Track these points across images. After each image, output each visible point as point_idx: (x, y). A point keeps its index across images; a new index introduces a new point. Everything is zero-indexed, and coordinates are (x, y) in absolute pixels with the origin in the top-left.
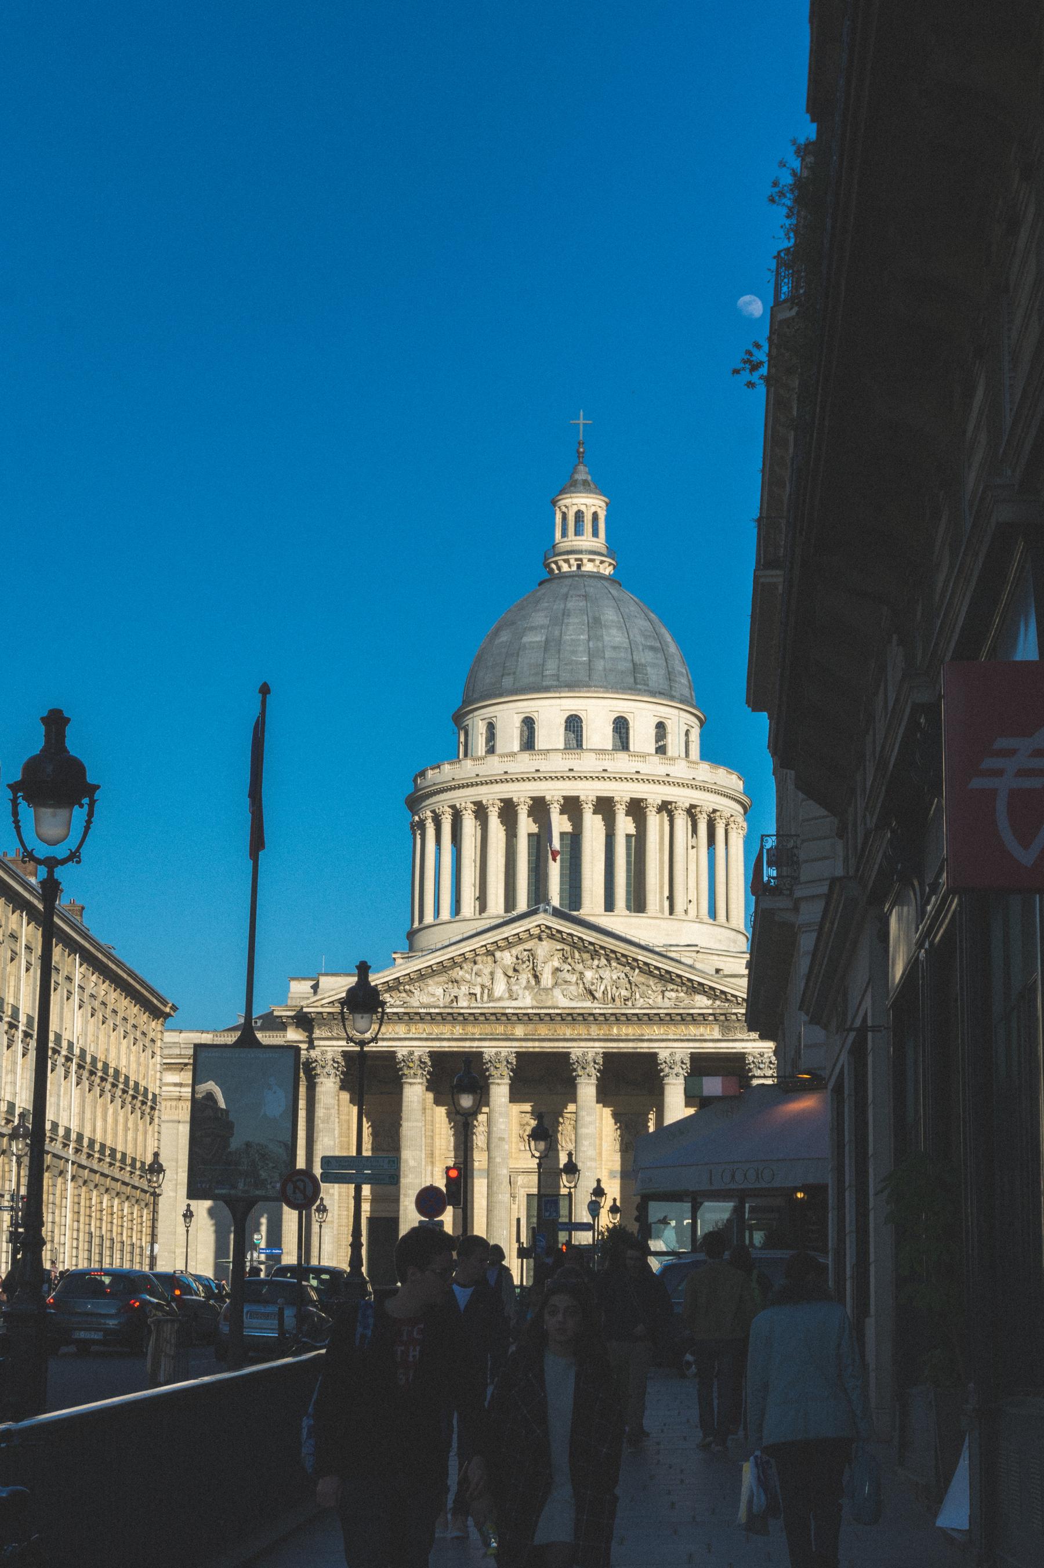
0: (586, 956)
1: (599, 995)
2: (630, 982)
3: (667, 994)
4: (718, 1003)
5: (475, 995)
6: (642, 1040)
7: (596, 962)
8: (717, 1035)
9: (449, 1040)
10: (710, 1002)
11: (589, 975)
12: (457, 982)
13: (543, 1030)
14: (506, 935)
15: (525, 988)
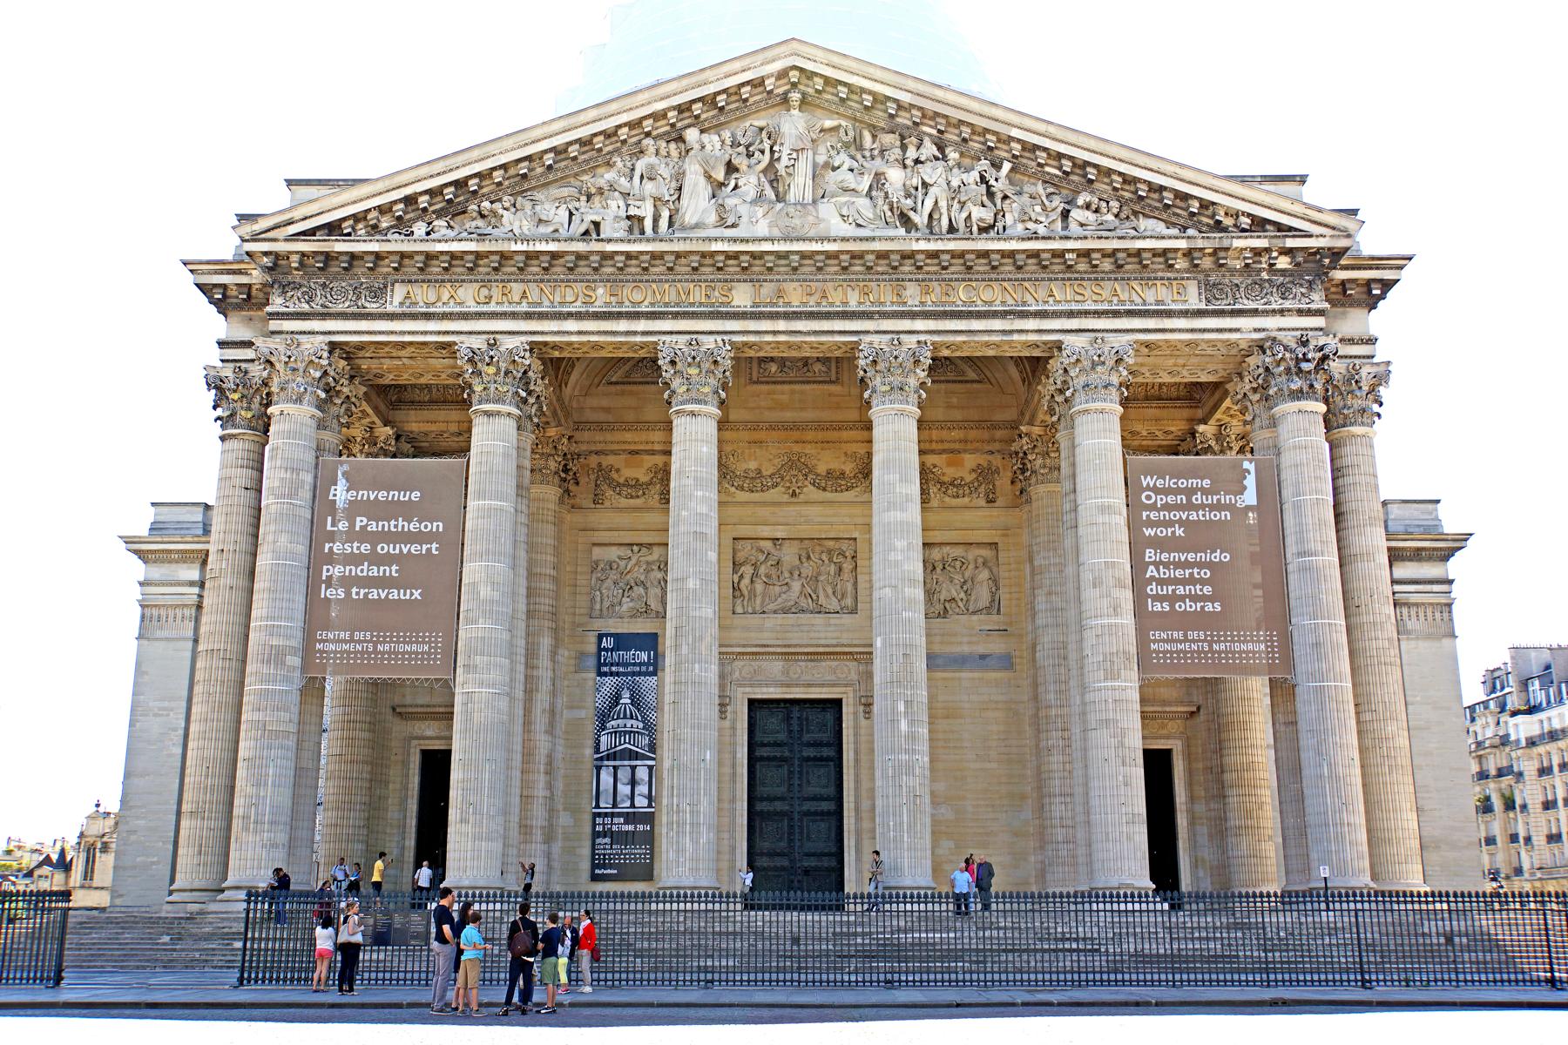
0: (890, 139)
1: (920, 219)
2: (990, 194)
3: (1076, 214)
4: (1191, 232)
5: (641, 220)
6: (1023, 315)
7: (912, 153)
8: (1194, 301)
9: (579, 316)
10: (1174, 232)
11: (895, 176)
12: (600, 191)
13: (796, 296)
14: (711, 89)
15: (754, 202)
